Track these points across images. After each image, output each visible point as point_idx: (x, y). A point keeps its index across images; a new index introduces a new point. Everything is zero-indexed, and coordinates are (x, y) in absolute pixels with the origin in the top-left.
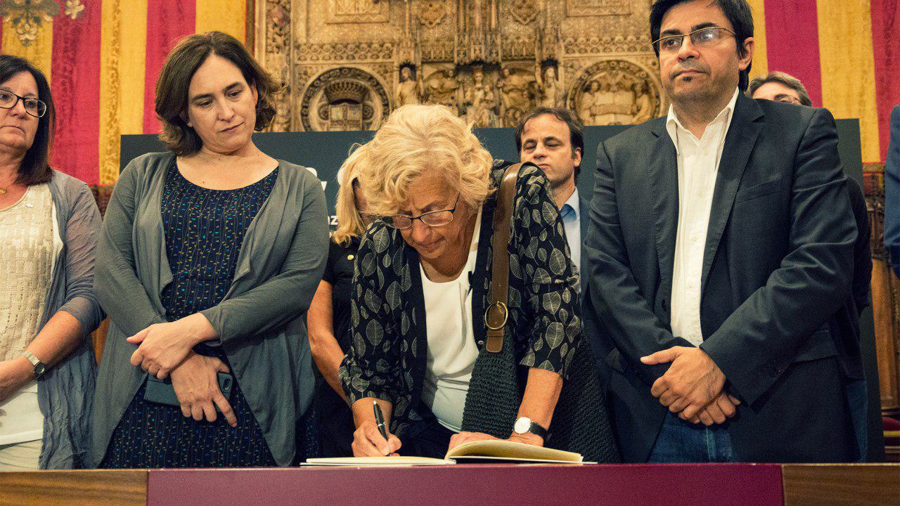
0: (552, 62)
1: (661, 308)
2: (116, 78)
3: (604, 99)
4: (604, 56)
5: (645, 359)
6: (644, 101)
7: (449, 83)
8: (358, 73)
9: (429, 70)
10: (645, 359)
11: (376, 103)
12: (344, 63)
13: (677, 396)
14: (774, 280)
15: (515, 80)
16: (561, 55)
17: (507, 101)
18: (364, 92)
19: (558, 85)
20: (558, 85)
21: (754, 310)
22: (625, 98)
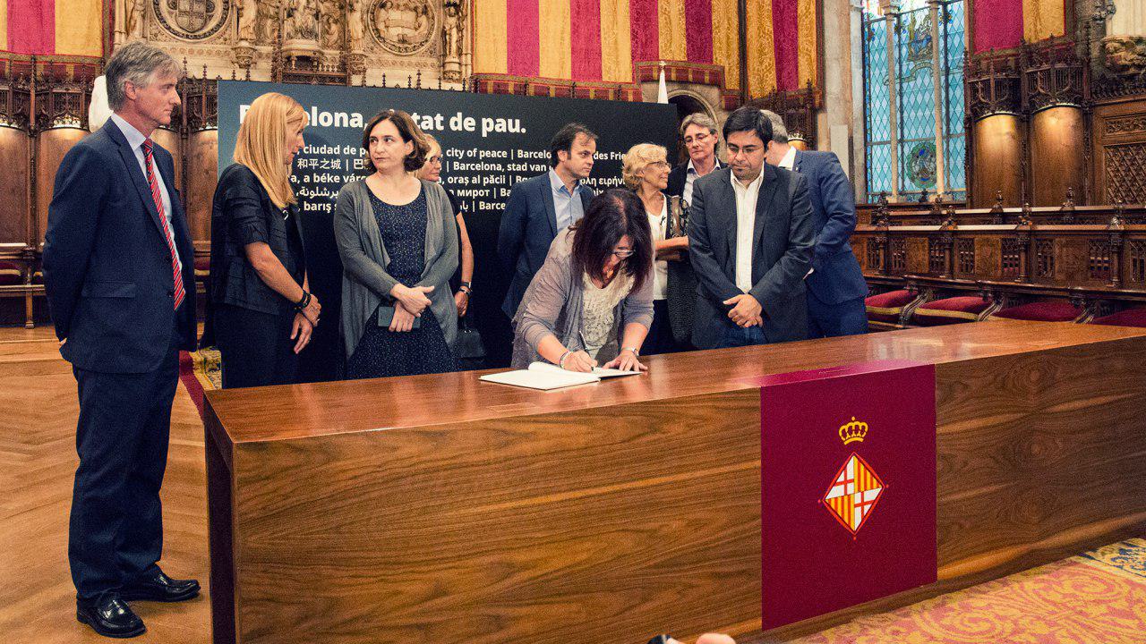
1: (731, 274)
5: (725, 302)
10: (725, 302)
13: (741, 317)
14: (784, 259)
21: (775, 274)
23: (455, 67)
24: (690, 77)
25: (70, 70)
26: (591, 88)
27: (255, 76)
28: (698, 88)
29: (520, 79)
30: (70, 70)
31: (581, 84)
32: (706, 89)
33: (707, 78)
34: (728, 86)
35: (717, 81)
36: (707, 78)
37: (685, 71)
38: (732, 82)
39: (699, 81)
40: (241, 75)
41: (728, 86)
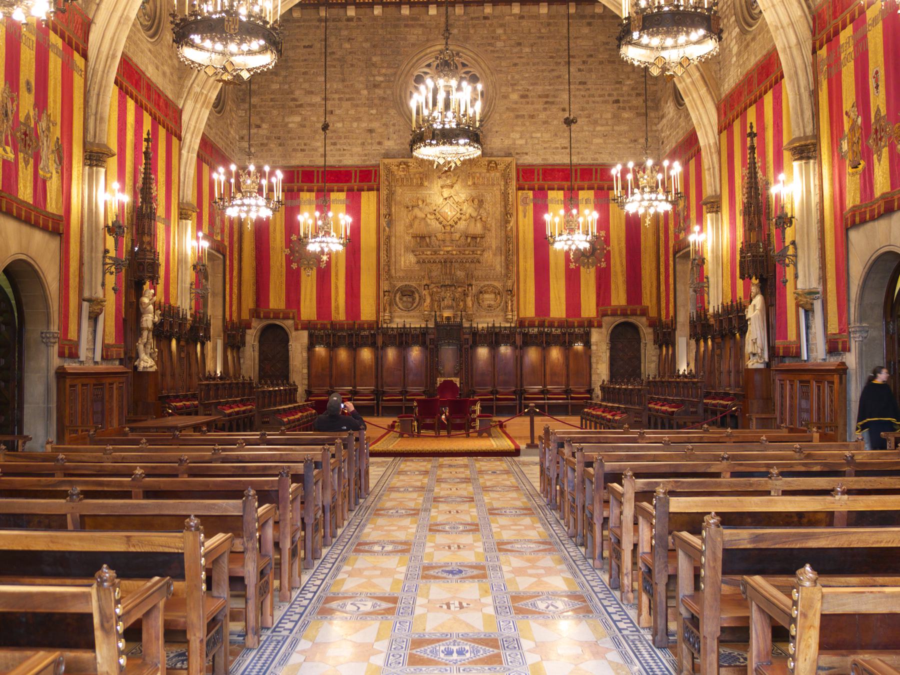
0: (471, 285)
2: (337, 288)
3: (486, 296)
4: (486, 283)
6: (498, 297)
7: (439, 290)
8: (411, 286)
9: (433, 285)
11: (417, 296)
12: (407, 283)
15: (459, 289)
16: (474, 282)
17: (457, 295)
18: (413, 292)
19: (474, 290)
20: (474, 290)
22: (493, 296)
23: (510, 317)
24: (629, 312)
25: (366, 326)
26: (576, 321)
27: (429, 326)
28: (635, 317)
29: (542, 318)
30: (366, 326)
31: (570, 319)
32: (639, 318)
33: (638, 312)
34: (651, 315)
35: (644, 312)
36: (638, 312)
37: (626, 310)
38: (653, 313)
39: (634, 313)
40: (423, 326)
41: (651, 315)
